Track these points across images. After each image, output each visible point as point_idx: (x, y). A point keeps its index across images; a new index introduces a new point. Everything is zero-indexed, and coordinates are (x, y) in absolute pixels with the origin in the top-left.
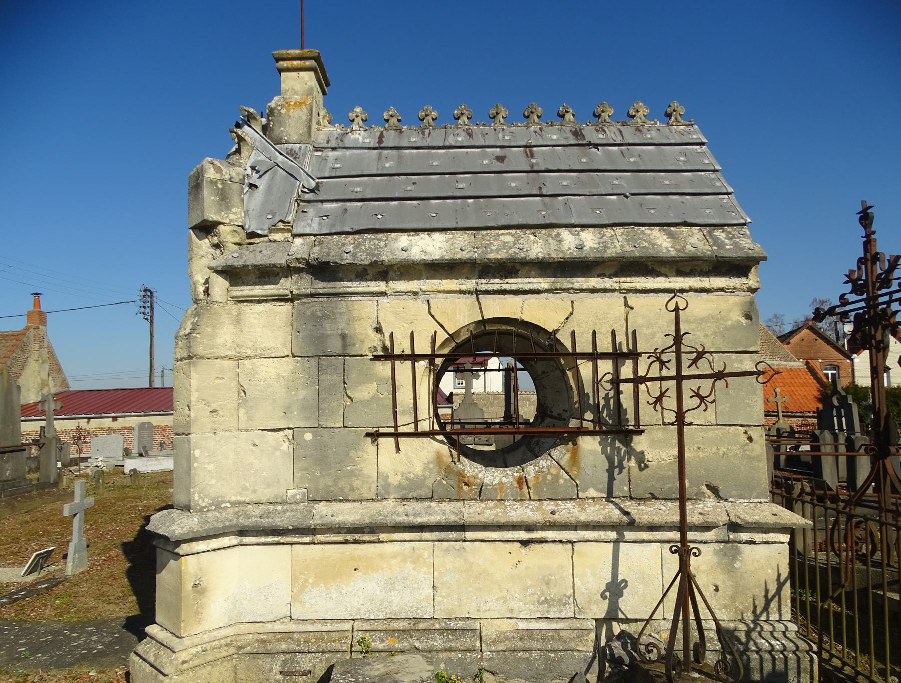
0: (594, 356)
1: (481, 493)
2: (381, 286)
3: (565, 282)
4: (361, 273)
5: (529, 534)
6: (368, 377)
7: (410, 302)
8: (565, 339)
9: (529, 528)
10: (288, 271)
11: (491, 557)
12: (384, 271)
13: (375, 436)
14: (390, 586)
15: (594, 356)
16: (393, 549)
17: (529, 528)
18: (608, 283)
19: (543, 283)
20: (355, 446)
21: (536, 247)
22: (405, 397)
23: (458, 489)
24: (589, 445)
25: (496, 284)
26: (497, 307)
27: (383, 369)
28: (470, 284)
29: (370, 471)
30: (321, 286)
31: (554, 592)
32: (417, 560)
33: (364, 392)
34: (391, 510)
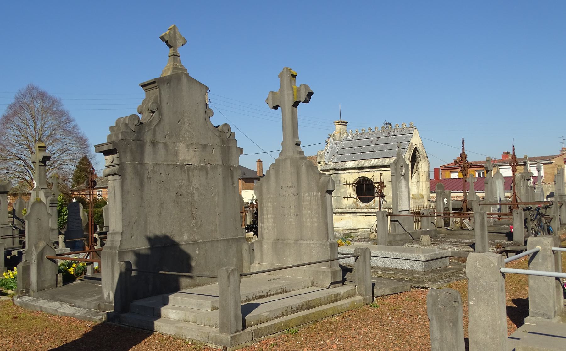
0: (377, 183)
1: (360, 207)
2: (344, 172)
3: (372, 170)
4: (342, 169)
5: (366, 214)
6: (343, 188)
7: (350, 175)
8: (372, 180)
9: (366, 213)
10: (331, 170)
11: (361, 218)
12: (345, 169)
13: (344, 198)
14: (347, 222)
15: (377, 183)
16: (347, 216)
17: (366, 213)
18: (378, 169)
19: (368, 170)
20: (342, 199)
21: (367, 163)
22: (348, 191)
23: (357, 206)
24: (377, 199)
25: (361, 170)
26: (362, 175)
27: (345, 186)
28: (357, 171)
29: (344, 203)
30: (336, 172)
31: (370, 224)
32: (350, 218)
33: (343, 190)
34: (347, 210)
